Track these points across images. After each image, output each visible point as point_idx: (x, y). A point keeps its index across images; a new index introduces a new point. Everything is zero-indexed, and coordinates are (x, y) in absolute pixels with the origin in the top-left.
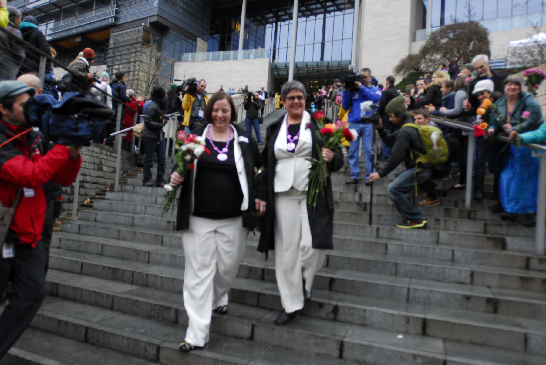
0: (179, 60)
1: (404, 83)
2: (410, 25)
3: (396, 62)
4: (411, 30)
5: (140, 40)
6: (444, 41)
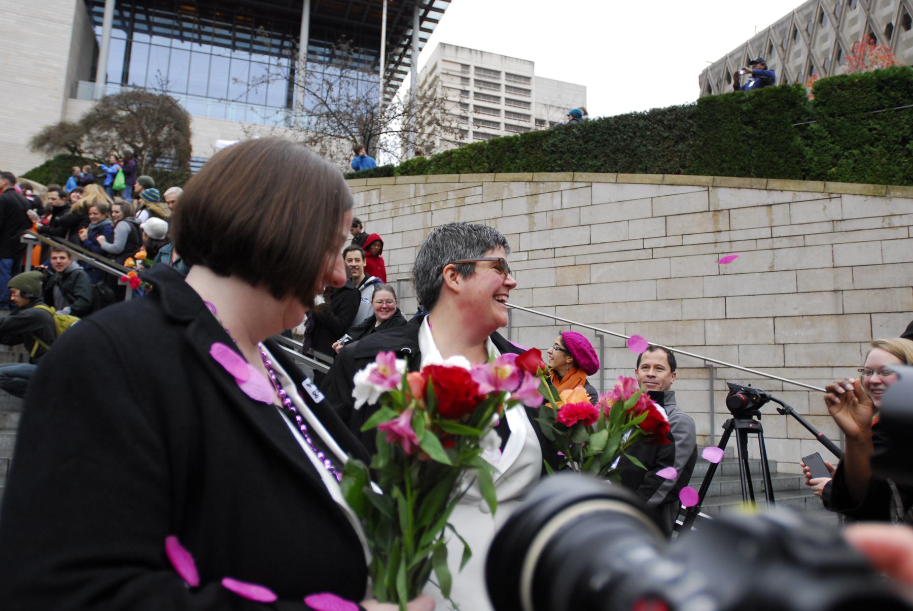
1: (47, 169)
2: (68, 69)
3: (37, 128)
4: (68, 77)
6: (123, 113)
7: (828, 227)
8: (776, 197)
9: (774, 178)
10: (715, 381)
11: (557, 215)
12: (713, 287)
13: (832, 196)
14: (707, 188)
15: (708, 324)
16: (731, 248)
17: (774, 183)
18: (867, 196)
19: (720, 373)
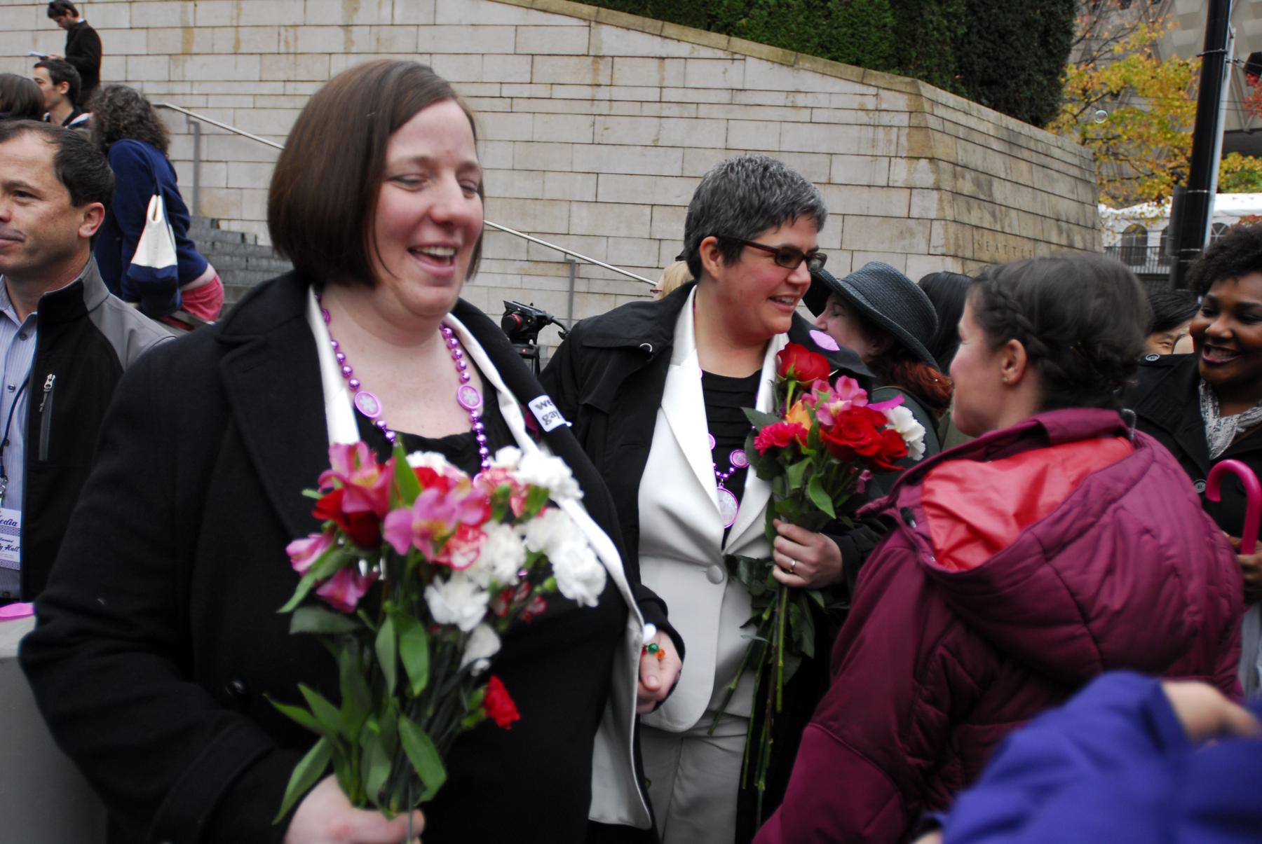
7: (725, 97)
8: (671, 48)
9: (672, 20)
10: (577, 281)
11: (385, 32)
12: (584, 158)
13: (736, 56)
14: (590, 22)
15: (575, 206)
16: (611, 109)
17: (672, 29)
18: (773, 62)
19: (584, 271)
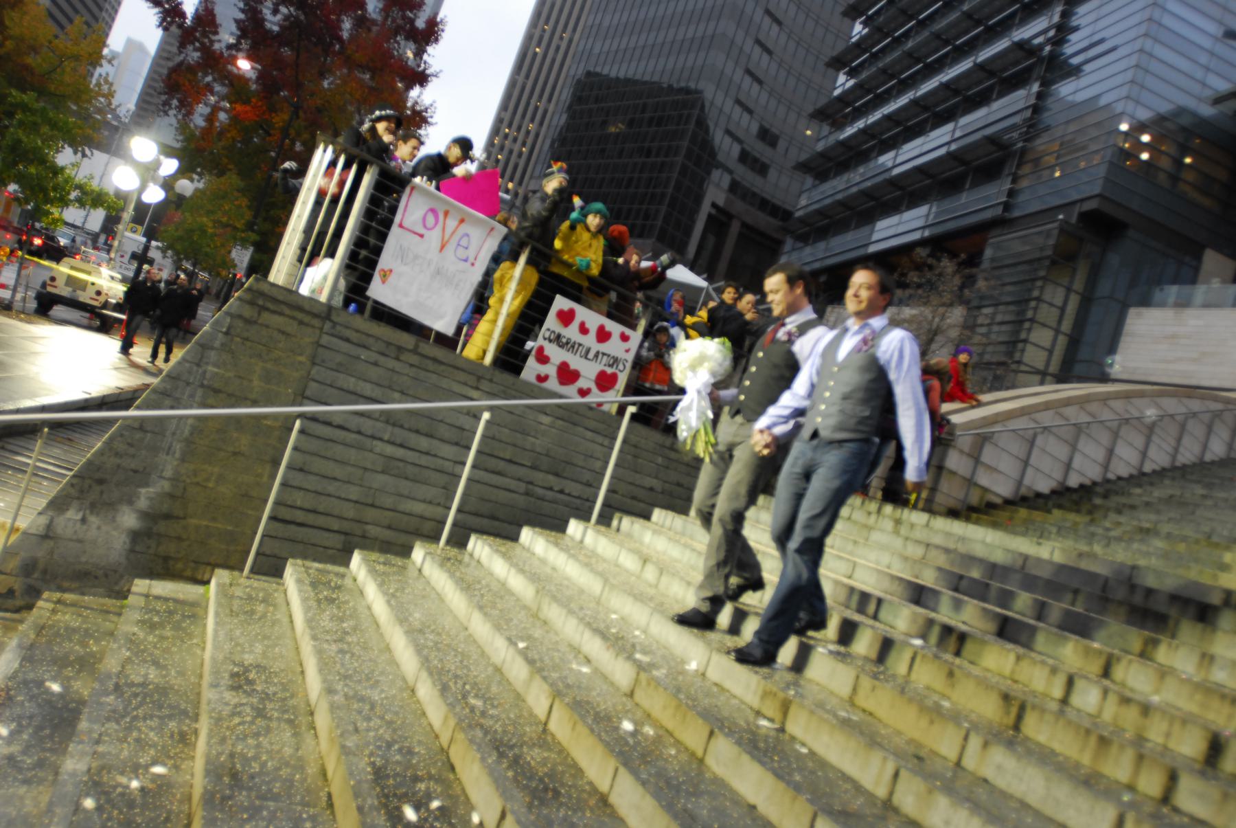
0: (1145, 302)
5: (1049, 252)
